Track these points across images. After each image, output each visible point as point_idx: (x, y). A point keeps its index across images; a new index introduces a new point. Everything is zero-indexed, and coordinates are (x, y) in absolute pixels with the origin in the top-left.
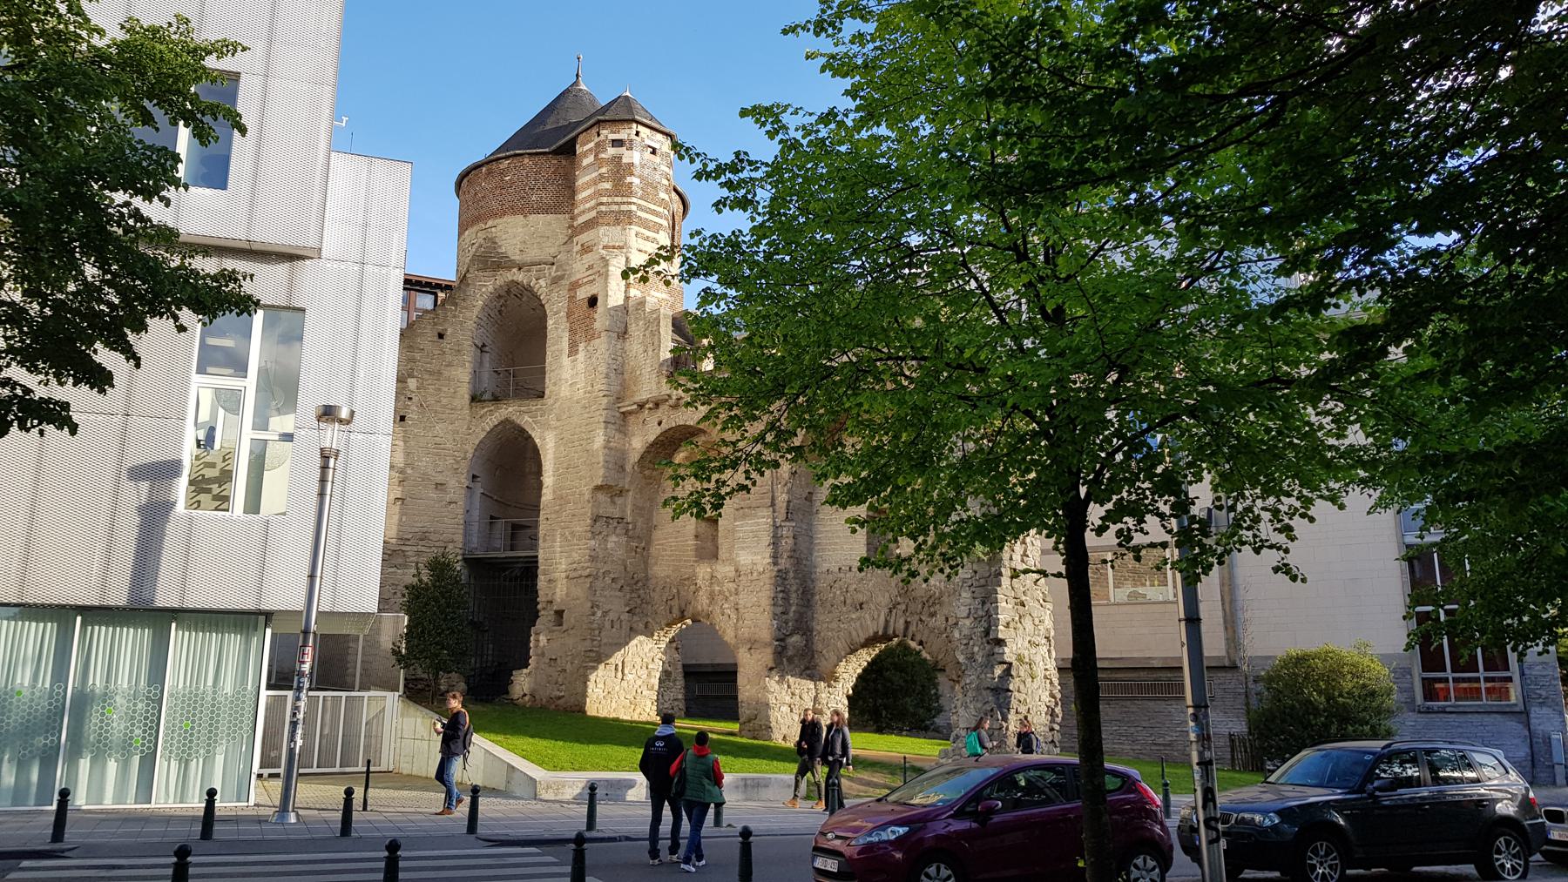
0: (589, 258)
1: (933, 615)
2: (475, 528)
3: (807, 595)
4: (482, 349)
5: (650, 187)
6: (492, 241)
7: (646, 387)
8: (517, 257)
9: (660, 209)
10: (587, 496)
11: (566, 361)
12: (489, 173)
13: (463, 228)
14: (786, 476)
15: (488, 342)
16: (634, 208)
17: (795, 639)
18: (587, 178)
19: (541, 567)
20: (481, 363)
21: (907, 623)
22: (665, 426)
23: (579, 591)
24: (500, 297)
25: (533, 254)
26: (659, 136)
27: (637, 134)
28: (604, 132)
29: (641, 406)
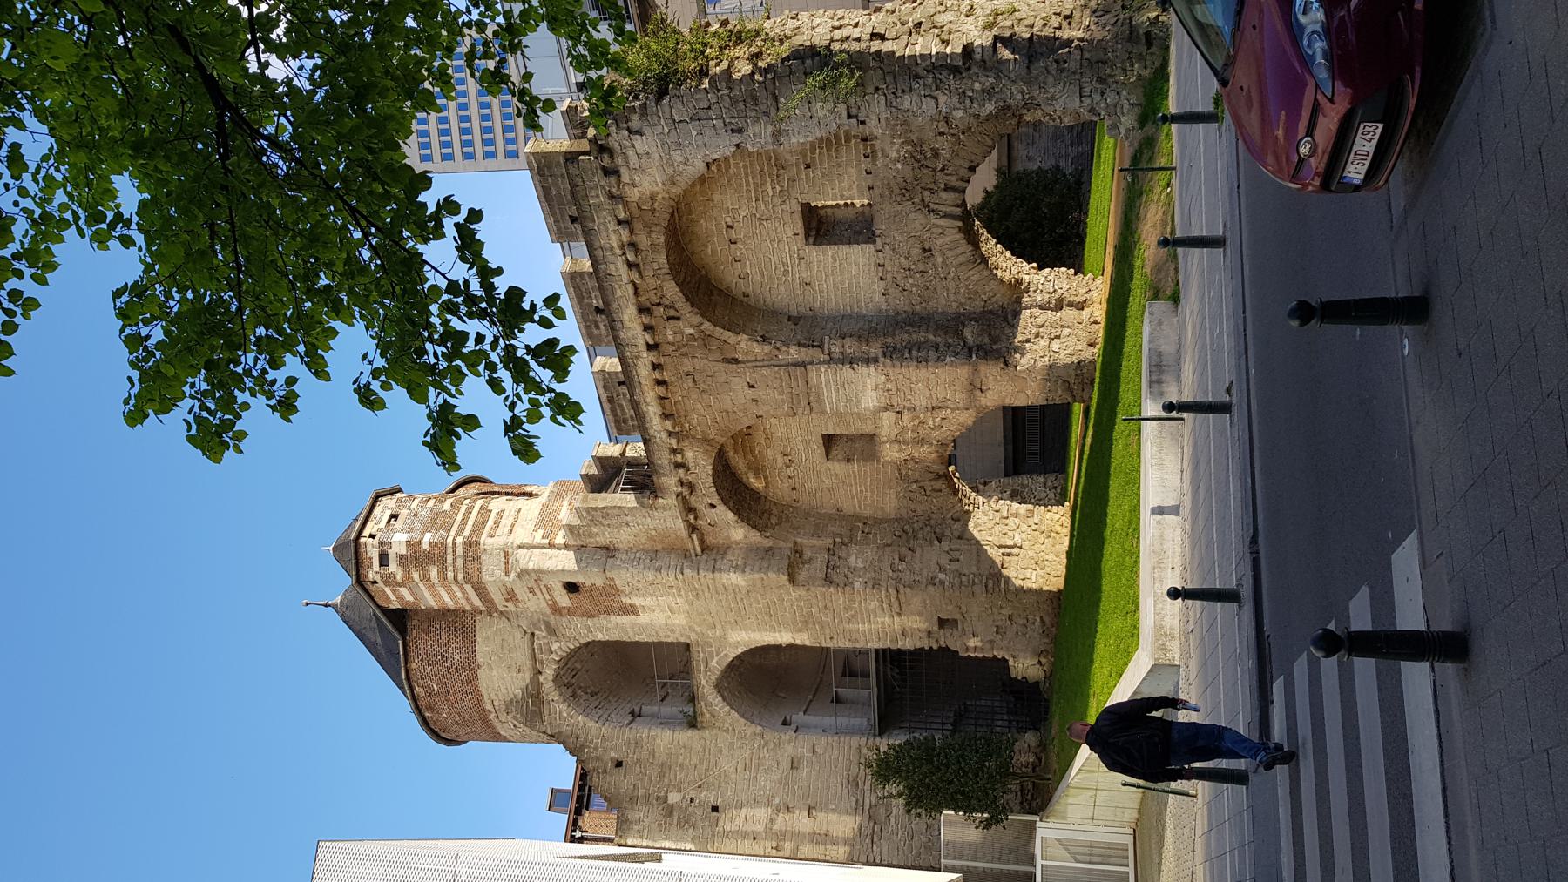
0: (521, 593)
1: (936, 154)
2: (843, 721)
3: (914, 320)
4: (635, 715)
5: (437, 521)
6: (509, 705)
7: (670, 523)
8: (527, 676)
9: (463, 508)
10: (802, 592)
11: (644, 619)
12: (431, 708)
13: (497, 737)
14: (767, 348)
15: (628, 708)
16: (459, 540)
18: (427, 595)
19: (889, 644)
20: (653, 716)
21: (947, 188)
22: (716, 500)
23: (916, 600)
24: (574, 695)
25: (522, 657)
26: (377, 510)
27: (372, 536)
28: (371, 576)
29: (693, 529)
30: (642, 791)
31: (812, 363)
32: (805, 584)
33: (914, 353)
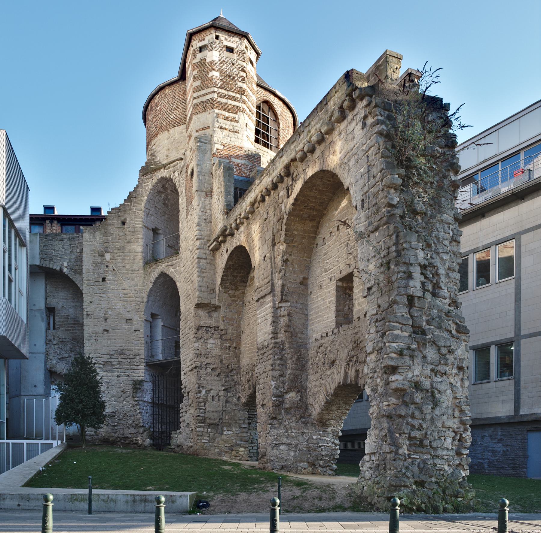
8: (164, 162)
17: (292, 396)
22: (229, 252)
30: (110, 238)
31: (274, 296)
32: (196, 315)
33: (278, 362)
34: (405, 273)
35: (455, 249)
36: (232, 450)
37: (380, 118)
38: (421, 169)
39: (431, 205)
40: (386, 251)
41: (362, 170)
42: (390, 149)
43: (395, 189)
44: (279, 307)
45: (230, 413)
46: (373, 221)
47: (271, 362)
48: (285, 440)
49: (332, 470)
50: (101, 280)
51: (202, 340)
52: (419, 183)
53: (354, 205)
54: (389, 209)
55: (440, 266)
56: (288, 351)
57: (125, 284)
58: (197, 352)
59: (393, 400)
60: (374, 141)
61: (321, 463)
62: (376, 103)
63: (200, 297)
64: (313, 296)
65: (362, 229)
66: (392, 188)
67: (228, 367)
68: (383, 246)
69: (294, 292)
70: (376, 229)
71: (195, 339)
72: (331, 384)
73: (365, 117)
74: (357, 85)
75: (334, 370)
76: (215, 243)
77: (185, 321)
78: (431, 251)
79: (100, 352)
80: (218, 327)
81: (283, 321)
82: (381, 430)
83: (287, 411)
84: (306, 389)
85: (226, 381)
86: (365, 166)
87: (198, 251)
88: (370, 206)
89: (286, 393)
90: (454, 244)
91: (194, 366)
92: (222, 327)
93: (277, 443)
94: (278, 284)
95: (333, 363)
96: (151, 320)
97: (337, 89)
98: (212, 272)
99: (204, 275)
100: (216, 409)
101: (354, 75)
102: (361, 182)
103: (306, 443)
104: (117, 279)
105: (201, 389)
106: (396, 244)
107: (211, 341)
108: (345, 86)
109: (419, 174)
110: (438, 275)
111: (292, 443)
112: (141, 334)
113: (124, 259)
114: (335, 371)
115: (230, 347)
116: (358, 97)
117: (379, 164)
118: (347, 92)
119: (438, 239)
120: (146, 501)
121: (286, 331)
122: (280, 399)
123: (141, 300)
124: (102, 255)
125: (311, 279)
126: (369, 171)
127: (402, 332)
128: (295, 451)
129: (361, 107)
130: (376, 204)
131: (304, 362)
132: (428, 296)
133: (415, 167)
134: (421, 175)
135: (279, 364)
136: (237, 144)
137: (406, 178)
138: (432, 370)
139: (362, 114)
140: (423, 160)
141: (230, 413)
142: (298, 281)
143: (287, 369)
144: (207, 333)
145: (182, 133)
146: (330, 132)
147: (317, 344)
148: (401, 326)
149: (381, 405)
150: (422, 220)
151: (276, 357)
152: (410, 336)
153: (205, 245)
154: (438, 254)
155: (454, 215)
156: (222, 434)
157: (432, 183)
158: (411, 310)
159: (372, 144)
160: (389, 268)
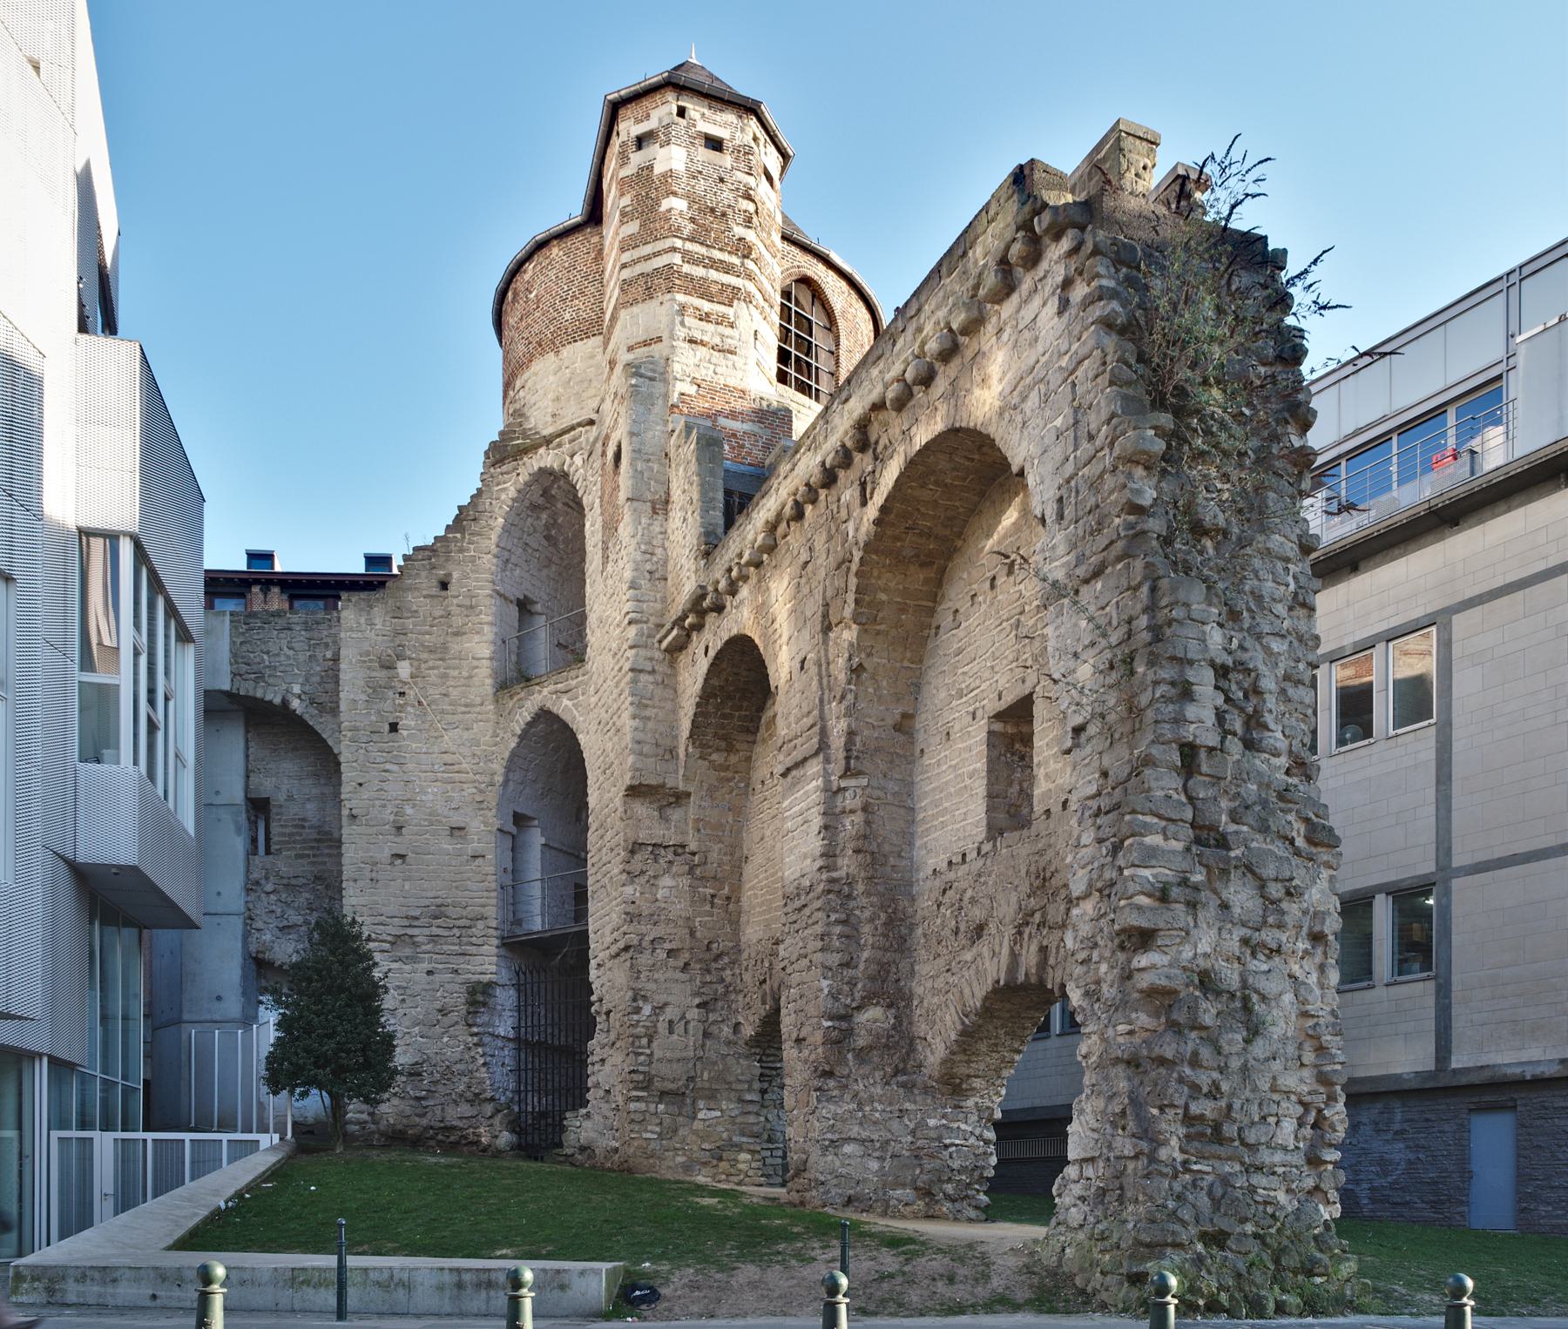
8: (546, 432)
17: (873, 1017)
22: (712, 653)
30: (409, 623)
31: (827, 761)
32: (627, 815)
33: (838, 929)
34: (1173, 684)
35: (1302, 626)
36: (720, 1159)
37: (1104, 282)
38: (1212, 418)
39: (1240, 511)
40: (1124, 629)
41: (1059, 422)
42: (1133, 362)
43: (1147, 468)
44: (840, 789)
45: (715, 1063)
46: (1088, 553)
47: (819, 929)
48: (855, 1130)
49: (977, 1208)
50: (387, 727)
51: (643, 879)
52: (1208, 453)
53: (1038, 512)
54: (1131, 518)
55: (1262, 668)
56: (864, 901)
57: (449, 741)
58: (630, 909)
59: (1143, 1019)
60: (1091, 343)
61: (949, 1188)
62: (1095, 245)
63: (637, 770)
64: (926, 761)
65: (1060, 575)
66: (1138, 463)
67: (708, 949)
68: (1114, 615)
69: (877, 750)
70: (1097, 574)
71: (624, 876)
72: (975, 984)
73: (1067, 284)
74: (1046, 198)
75: (983, 947)
76: (675, 632)
77: (601, 832)
78: (1242, 629)
79: (383, 910)
80: (683, 847)
81: (851, 825)
82: (1111, 1098)
83: (862, 1055)
84: (910, 998)
85: (704, 984)
86: (1067, 410)
87: (633, 651)
88: (1081, 513)
89: (858, 1008)
90: (1301, 612)
91: (621, 944)
92: (693, 846)
93: (836, 1136)
94: (838, 729)
95: (980, 930)
96: (514, 830)
97: (991, 212)
98: (669, 705)
99: (648, 713)
100: (678, 1055)
101: (1037, 175)
102: (1057, 452)
103: (910, 1138)
104: (427, 726)
105: (641, 1003)
106: (1151, 608)
107: (667, 881)
108: (1012, 206)
109: (1208, 432)
110: (1257, 692)
111: (875, 1137)
112: (489, 866)
113: (445, 676)
114: (986, 952)
115: (713, 896)
116: (1047, 231)
117: (1103, 401)
118: (1020, 219)
119: (1259, 598)
120: (490, 1285)
121: (857, 851)
122: (844, 1025)
123: (487, 779)
124: (389, 666)
125: (924, 716)
126: (1076, 422)
127: (1166, 839)
128: (881, 1159)
129: (1055, 257)
130: (1097, 506)
131: (904, 931)
132: (1235, 746)
133: (1198, 411)
134: (1212, 434)
135: (840, 936)
136: (732, 382)
137: (1175, 437)
138: (1245, 941)
139: (1059, 275)
140: (1216, 393)
141: (715, 1063)
142: (890, 722)
143: (861, 948)
144: (656, 861)
145: (592, 357)
146: (973, 327)
147: (938, 883)
148: (1163, 823)
149: (1110, 1032)
150: (1216, 549)
151: (833, 917)
152: (1188, 849)
153: (649, 636)
154: (1259, 637)
155: (1300, 537)
156: (694, 1118)
157: (1242, 454)
158: (1191, 783)
159: (1084, 351)
160: (1132, 673)
